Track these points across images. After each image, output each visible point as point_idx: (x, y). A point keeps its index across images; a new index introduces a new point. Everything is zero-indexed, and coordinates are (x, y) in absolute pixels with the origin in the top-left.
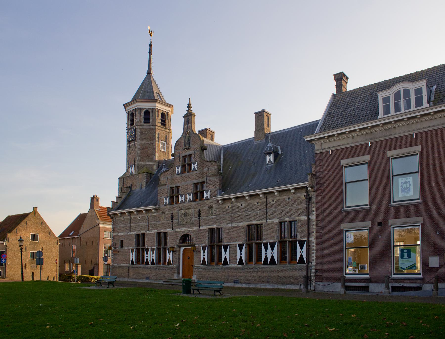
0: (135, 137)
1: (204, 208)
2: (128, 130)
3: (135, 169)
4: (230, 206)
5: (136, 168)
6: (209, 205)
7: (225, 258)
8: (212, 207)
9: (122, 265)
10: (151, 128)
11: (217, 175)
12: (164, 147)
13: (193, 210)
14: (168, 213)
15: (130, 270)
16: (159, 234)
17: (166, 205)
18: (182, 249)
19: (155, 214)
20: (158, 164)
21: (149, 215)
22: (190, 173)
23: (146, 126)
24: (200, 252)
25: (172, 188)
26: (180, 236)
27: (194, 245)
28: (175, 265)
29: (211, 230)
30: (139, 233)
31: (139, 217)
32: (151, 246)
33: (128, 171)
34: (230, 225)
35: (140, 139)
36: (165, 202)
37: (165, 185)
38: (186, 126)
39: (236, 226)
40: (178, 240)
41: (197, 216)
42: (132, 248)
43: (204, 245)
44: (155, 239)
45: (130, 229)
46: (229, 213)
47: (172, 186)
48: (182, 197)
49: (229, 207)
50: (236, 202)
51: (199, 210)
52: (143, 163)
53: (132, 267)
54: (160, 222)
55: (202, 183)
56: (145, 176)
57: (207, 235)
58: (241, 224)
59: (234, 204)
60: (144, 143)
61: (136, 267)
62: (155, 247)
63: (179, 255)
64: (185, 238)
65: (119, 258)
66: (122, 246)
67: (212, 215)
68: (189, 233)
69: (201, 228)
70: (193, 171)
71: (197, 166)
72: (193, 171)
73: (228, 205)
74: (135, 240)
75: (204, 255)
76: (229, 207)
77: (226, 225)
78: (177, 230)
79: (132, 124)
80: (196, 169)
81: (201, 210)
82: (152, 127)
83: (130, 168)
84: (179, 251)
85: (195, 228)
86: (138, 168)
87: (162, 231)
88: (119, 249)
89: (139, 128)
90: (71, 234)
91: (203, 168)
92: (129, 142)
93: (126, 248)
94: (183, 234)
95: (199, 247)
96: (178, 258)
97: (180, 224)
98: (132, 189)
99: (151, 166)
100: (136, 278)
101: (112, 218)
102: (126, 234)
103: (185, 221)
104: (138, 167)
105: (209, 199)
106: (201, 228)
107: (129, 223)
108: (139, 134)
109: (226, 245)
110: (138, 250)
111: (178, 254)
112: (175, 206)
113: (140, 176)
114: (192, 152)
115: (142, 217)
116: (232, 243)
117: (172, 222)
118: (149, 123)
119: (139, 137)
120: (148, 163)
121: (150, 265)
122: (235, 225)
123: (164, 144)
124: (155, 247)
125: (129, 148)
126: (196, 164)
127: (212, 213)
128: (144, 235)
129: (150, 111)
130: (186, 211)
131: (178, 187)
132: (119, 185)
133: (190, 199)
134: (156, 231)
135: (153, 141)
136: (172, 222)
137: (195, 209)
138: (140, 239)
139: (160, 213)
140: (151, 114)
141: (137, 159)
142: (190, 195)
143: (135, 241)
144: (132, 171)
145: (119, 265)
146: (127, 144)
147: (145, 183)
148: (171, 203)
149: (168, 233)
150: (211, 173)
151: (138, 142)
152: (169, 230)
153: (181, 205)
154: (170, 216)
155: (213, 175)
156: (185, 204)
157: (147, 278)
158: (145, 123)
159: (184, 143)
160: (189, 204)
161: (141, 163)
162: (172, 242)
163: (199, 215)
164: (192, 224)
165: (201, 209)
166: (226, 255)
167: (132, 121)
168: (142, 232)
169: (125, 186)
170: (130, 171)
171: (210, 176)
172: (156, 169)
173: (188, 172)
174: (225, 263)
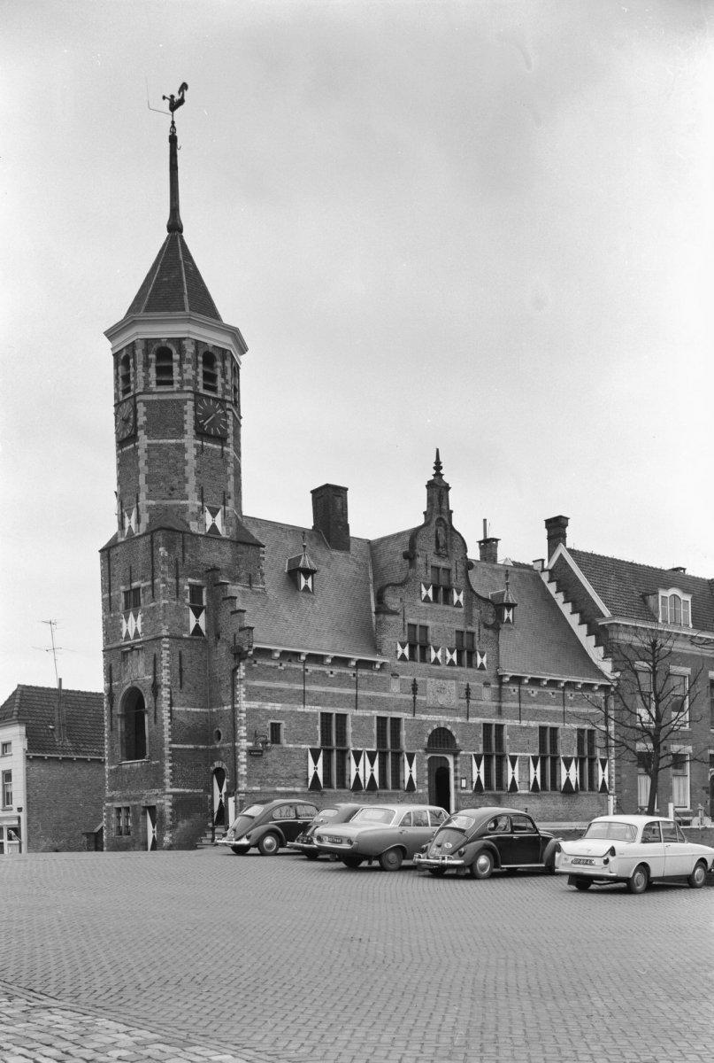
16: (382, 720)
26: (430, 732)
51: (468, 685)
58: (533, 724)
68: (449, 728)
69: (472, 720)
78: (424, 717)
85: (459, 720)
94: (435, 727)
106: (472, 720)
115: (340, 675)
134: (376, 713)
136: (415, 698)
138: (333, 727)
152: (405, 716)
160: (449, 669)
165: (471, 684)
168: (341, 711)
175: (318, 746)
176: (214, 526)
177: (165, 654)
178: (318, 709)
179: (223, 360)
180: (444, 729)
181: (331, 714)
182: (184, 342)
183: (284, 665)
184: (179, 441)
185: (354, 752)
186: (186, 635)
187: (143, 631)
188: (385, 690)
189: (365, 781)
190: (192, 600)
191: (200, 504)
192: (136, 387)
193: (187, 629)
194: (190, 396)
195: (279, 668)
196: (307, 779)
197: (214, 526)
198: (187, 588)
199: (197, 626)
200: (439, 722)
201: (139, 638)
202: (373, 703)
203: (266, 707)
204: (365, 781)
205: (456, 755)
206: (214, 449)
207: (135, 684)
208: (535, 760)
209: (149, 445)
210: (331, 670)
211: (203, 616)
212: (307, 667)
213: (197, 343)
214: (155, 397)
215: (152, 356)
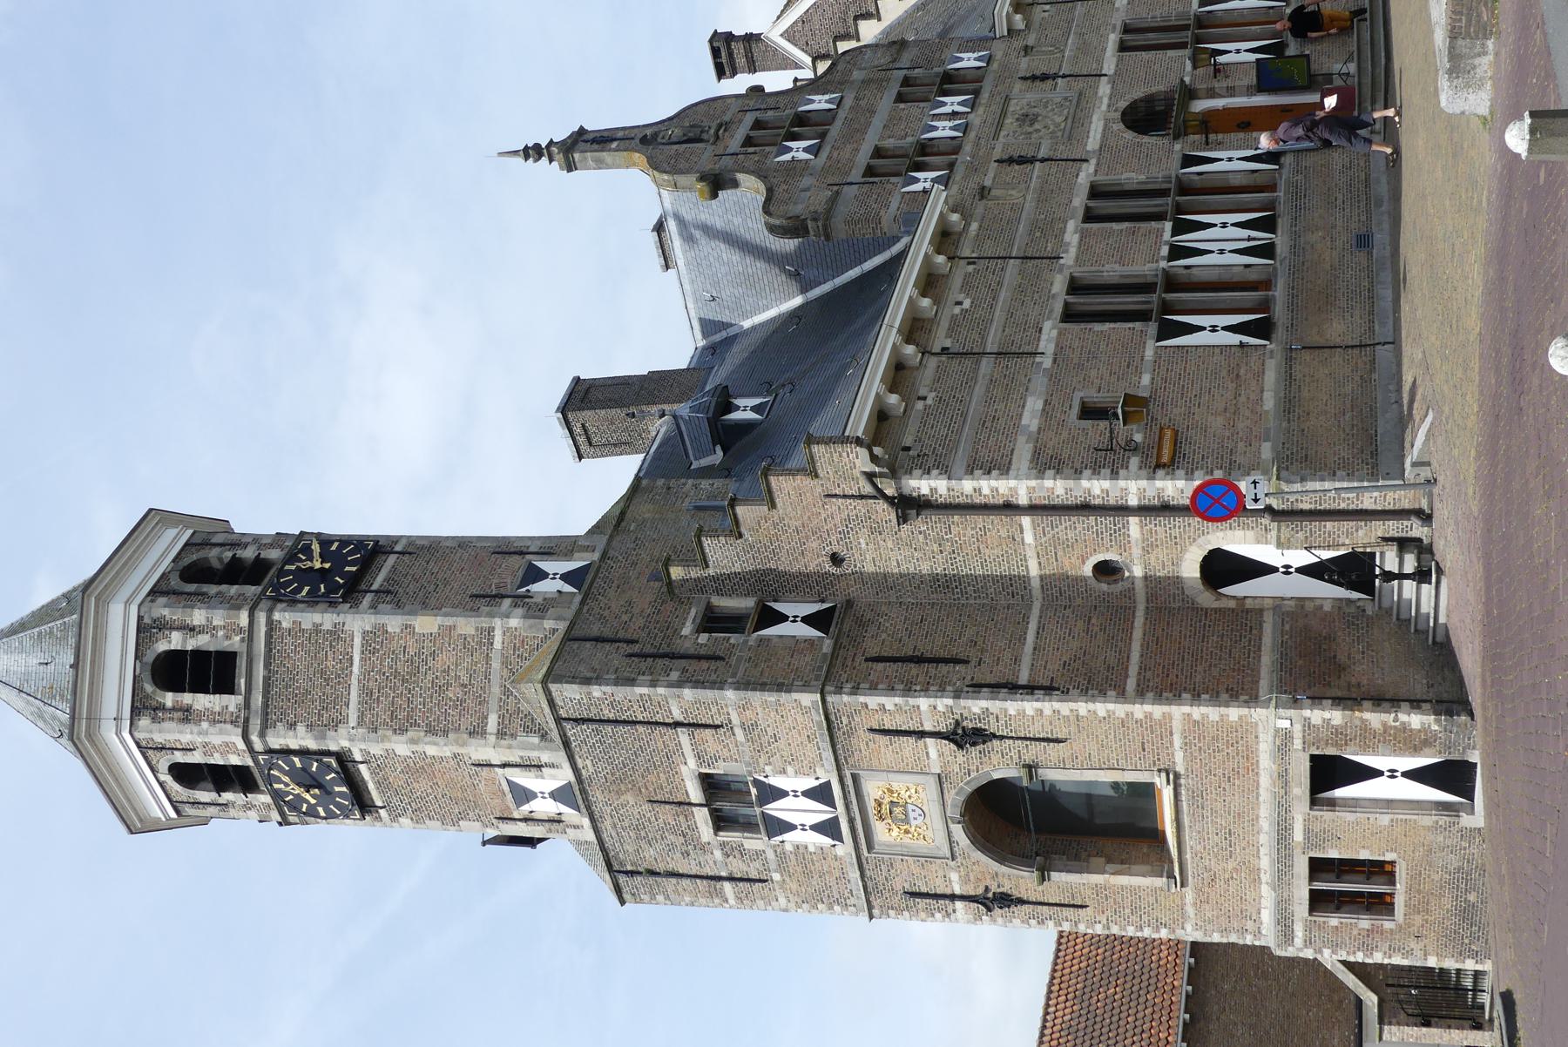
9: (1269, 402)
19: (974, 226)
30: (1058, 308)
31: (959, 301)
53: (1291, 328)
61: (1292, 306)
65: (1217, 423)
68: (1123, 104)
69: (1109, 66)
78: (1093, 143)
85: (1104, 88)
87: (1079, 201)
93: (1146, 379)
102: (1039, 383)
106: (1109, 66)
115: (966, 287)
121: (1281, 240)
149: (1100, 178)
152: (1085, 175)
157: (1364, 241)
168: (1059, 285)
175: (1152, 328)
176: (566, 577)
177: (873, 701)
178: (1050, 333)
179: (206, 544)
180: (1124, 114)
181: (1066, 304)
182: (147, 620)
183: (922, 392)
184: (358, 641)
185: (1171, 258)
186: (828, 645)
187: (811, 770)
189: (1249, 239)
190: (740, 630)
191: (507, 602)
192: (228, 748)
193: (810, 642)
194: (261, 618)
195: (929, 401)
196: (1242, 345)
197: (566, 577)
198: (703, 638)
199: (807, 620)
200: (1107, 121)
201: (828, 784)
202: (1049, 227)
203: (1034, 427)
204: (1249, 239)
205: (1190, 93)
206: (394, 569)
207: (955, 799)
209: (361, 722)
211: (780, 607)
212: (937, 349)
213: (155, 592)
214: (257, 699)
215: (169, 699)
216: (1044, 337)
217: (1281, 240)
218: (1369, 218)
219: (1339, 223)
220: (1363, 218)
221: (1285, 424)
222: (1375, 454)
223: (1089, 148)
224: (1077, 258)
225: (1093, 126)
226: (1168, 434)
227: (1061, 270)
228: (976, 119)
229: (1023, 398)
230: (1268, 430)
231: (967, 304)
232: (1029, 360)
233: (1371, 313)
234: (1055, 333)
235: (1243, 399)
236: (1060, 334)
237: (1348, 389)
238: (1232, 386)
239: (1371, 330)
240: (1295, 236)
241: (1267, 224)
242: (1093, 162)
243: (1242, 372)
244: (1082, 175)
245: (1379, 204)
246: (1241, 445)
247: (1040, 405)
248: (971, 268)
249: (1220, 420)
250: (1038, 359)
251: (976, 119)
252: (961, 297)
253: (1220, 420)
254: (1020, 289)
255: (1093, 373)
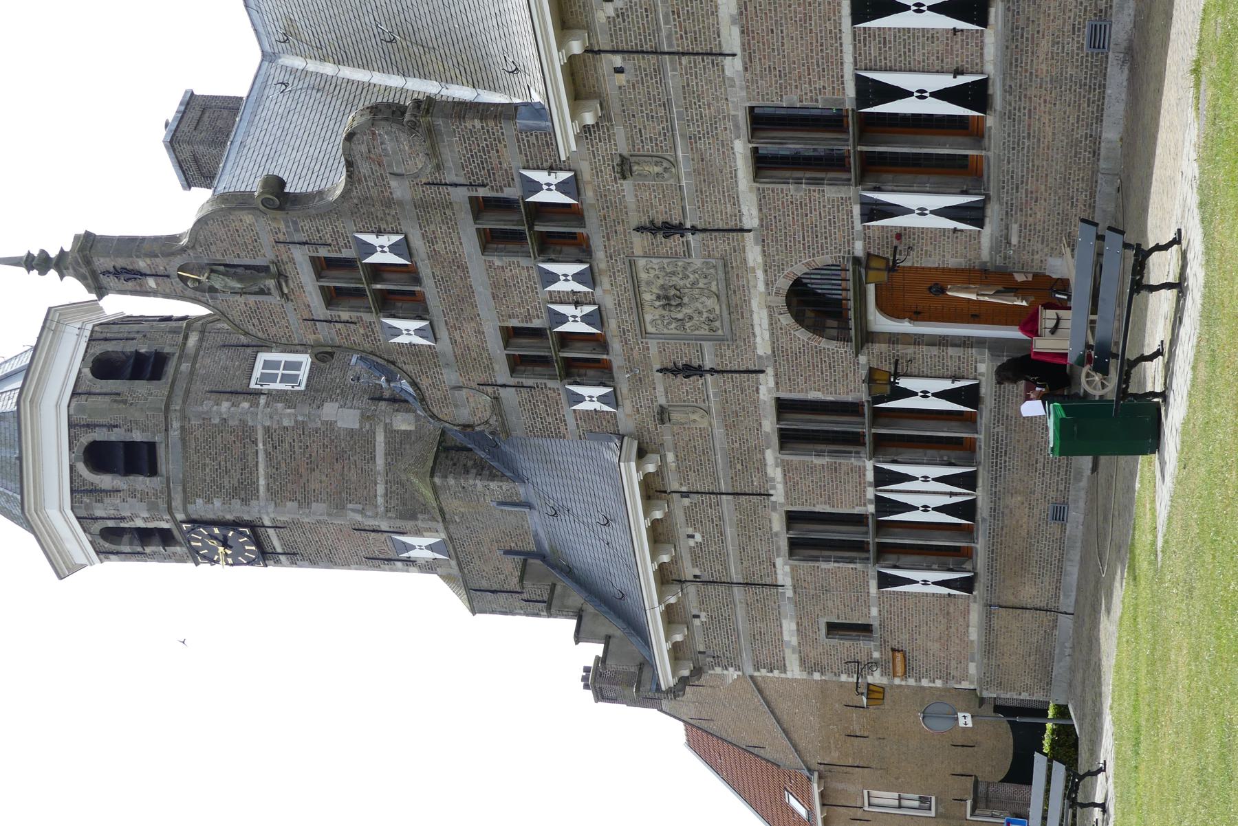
0: (235, 524)
1: (630, 199)
2: (195, 556)
3: (418, 533)
4: (618, 60)
5: (409, 525)
6: (608, 174)
7: (940, 95)
8: (624, 161)
9: (974, 634)
10: (183, 441)
11: (431, 133)
12: (289, 365)
13: (641, 263)
14: (661, 390)
15: (1010, 599)
17: (613, 399)
18: (881, 323)
19: (670, 457)
20: (383, 405)
21: (675, 485)
22: (425, 270)
23: (169, 461)
24: (900, 234)
25: (517, 364)
26: (802, 335)
27: (856, 261)
28: (982, 368)
29: (763, 164)
31: (690, 538)
32: (862, 486)
33: (428, 567)
34: (733, 67)
35: (245, 501)
36: (597, 406)
37: (496, 399)
38: (151, 283)
39: (736, 31)
40: (824, 343)
41: (675, 242)
42: (873, 584)
43: (857, 210)
44: (818, 461)
45: (760, 585)
46: (659, 69)
47: (502, 373)
48: (563, 319)
49: (619, 70)
50: (588, 28)
51: (640, 229)
52: (380, 489)
53: (990, 588)
54: (719, 432)
55: (481, 207)
56: (451, 481)
57: (793, 192)
59: (603, 42)
60: (269, 476)
61: (991, 568)
62: (869, 465)
63: (917, 340)
64: (812, 304)
65: (935, 647)
66: (865, 629)
67: (674, 164)
68: (784, 284)
69: (751, 219)
70: (410, 254)
71: (379, 232)
72: (410, 254)
73: (612, 75)
74: (824, 565)
75: (921, 209)
76: (619, 70)
77: (737, 87)
78: (763, 345)
79: (165, 538)
80: (396, 238)
81: (645, 220)
82: (175, 434)
83: (413, 554)
84: (893, 338)
85: (754, 255)
86: (410, 512)
87: (769, 424)
88: (881, 647)
89: (186, 501)
90: (802, 811)
91: (389, 202)
92: (265, 555)
93: (874, 611)
94: (786, 320)
95: (866, 238)
96: (934, 351)
97: (733, 326)
98: (532, 547)
99: (398, 442)
100: (1060, 571)
101: (698, 671)
102: (788, 608)
103: (711, 303)
104: (402, 516)
105: (575, 175)
106: (751, 219)
107: (722, 589)
108: (217, 503)
109: (858, 92)
110: (883, 551)
111: (910, 350)
112: (616, 355)
113: (453, 505)
114: (301, 256)
115: (690, 520)
116: (848, 58)
117: (713, 371)
118: (152, 446)
119: (236, 503)
120: (380, 461)
121: (981, 495)
122: (732, 39)
123: (267, 364)
124: (869, 465)
125: (294, 556)
126: (370, 238)
127: (659, 159)
128: (793, 518)
129: (86, 439)
130: (647, 297)
131: (510, 335)
132: (512, 613)
133: (577, 277)
134: (770, 456)
135: (253, 429)
136: (713, 371)
137: (638, 251)
139: (666, 434)
140: (100, 435)
141: (359, 517)
142: (554, 278)
143: (832, 565)
144: (430, 548)
145: (976, 649)
146: (278, 562)
147: (494, 485)
148: (600, 371)
150: (419, 163)
151: (264, 511)
152: (766, 389)
153: (612, 324)
154: (680, 379)
155: (433, 152)
156: (609, 302)
157: (1059, 514)
158: (153, 471)
159: (252, 299)
161: (380, 500)
162: (837, 374)
163: (670, 229)
164: (730, 274)
165: (635, 219)
166: (921, 93)
167: (145, 536)
168: (778, 523)
169: (514, 583)
170: (430, 555)
171: (438, 167)
172: (411, 416)
173: (417, 280)
174: (975, 96)
183: (695, 612)
188: (707, 435)
189: (951, 494)
196: (949, 595)
204: (951, 494)
208: (886, 581)
210: (682, 536)
216: (779, 571)
217: (981, 495)
218: (1067, 489)
219: (1038, 489)
220: (1062, 487)
221: (985, 661)
222: (1049, 683)
223: (760, 352)
224: (786, 493)
225: (755, 317)
226: (899, 656)
227: (774, 508)
228: (606, 294)
229: (779, 619)
230: (973, 655)
231: (698, 537)
232: (773, 590)
233: (1059, 581)
234: (787, 568)
235: (953, 630)
236: (792, 570)
237: (1035, 639)
238: (944, 621)
239: (1057, 596)
240: (995, 497)
241: (968, 481)
242: (770, 371)
243: (951, 610)
244: (763, 389)
245: (1078, 478)
246: (953, 663)
247: (794, 626)
248: (686, 501)
249: (937, 646)
250: (780, 590)
251: (606, 294)
252: (690, 531)
253: (937, 646)
254: (742, 525)
255: (830, 603)
